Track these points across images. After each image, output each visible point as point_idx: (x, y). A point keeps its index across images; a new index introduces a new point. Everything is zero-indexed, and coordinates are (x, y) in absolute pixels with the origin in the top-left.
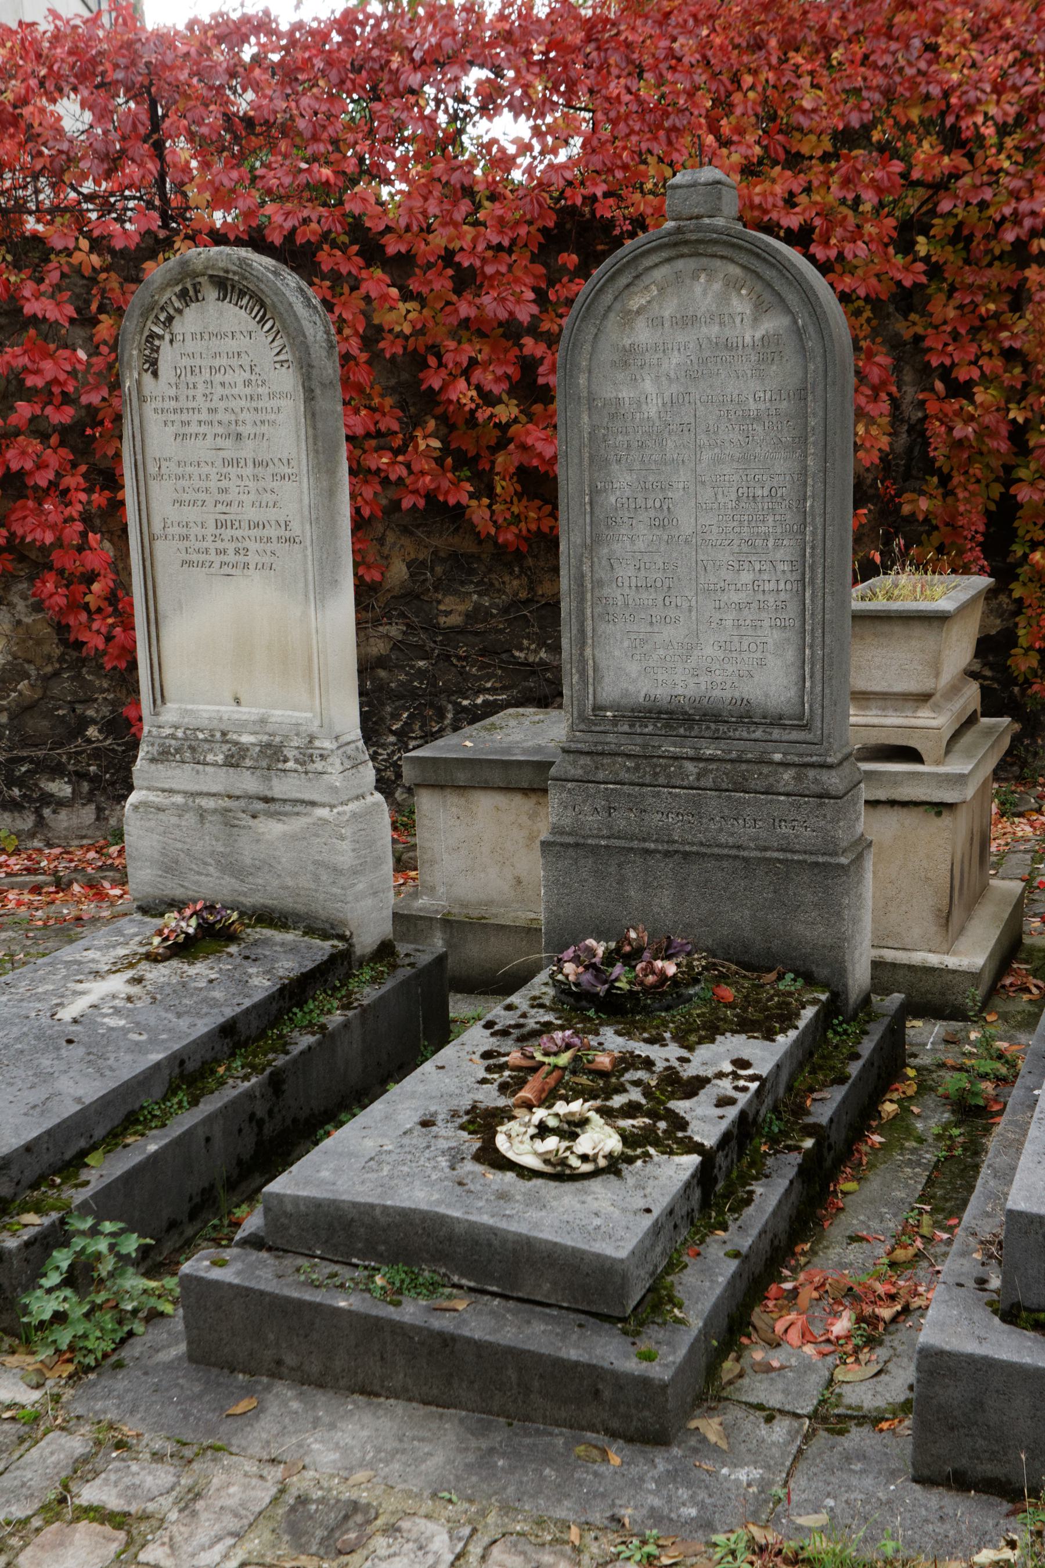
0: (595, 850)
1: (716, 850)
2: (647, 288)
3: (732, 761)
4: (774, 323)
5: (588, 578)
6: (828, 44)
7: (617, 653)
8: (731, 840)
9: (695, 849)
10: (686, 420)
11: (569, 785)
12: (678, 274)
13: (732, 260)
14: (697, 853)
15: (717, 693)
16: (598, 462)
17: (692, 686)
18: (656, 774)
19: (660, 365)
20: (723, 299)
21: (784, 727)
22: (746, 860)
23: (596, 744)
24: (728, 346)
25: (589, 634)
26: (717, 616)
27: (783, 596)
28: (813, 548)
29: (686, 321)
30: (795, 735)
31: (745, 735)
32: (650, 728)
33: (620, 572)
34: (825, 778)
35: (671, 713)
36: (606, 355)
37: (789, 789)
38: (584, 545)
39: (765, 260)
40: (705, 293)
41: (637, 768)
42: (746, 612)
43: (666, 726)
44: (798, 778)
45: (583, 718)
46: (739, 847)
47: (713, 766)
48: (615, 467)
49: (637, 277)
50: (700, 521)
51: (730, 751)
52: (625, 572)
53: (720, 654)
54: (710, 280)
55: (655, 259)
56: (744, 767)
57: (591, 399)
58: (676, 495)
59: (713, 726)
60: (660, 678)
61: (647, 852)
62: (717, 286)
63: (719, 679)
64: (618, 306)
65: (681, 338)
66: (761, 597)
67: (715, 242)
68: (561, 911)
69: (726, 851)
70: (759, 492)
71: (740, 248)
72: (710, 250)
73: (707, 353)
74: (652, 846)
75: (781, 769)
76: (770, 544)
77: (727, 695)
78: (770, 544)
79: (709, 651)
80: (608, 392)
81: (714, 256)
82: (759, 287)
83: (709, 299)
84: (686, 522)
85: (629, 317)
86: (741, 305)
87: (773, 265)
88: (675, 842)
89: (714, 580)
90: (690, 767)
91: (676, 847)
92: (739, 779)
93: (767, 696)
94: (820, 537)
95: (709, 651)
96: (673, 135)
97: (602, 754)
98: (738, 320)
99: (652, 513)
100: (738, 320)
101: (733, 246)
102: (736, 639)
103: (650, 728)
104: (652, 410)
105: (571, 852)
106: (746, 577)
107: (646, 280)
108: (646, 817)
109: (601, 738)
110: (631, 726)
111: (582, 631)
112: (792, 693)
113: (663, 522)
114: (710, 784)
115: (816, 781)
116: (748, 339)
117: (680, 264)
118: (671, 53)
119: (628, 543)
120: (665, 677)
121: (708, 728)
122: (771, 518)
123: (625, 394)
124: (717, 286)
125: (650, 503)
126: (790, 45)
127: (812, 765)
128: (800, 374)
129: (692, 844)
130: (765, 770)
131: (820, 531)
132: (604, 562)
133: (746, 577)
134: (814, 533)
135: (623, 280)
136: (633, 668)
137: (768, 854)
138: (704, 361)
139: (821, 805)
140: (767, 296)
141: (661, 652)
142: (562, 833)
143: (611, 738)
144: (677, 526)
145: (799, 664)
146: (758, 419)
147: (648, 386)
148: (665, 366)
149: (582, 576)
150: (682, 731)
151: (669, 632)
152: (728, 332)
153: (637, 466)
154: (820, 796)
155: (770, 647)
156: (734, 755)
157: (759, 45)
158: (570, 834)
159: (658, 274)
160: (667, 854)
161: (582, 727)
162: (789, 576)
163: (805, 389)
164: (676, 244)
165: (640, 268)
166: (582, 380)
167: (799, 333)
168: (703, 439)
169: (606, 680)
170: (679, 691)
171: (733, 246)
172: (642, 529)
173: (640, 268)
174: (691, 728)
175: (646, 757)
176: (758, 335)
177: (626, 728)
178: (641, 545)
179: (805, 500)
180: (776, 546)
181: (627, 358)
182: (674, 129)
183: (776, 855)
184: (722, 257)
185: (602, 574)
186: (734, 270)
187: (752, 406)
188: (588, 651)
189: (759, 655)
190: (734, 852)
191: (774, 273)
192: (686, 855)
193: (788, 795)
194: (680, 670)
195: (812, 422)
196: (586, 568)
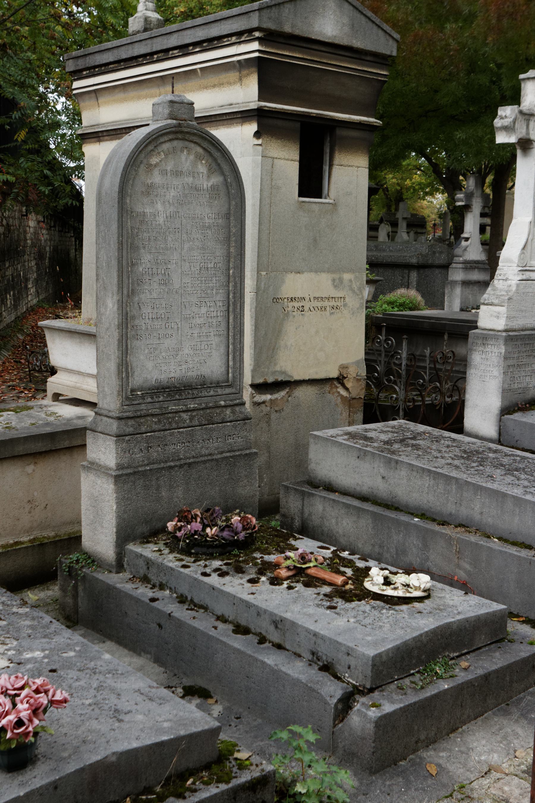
0: (144, 474)
1: (203, 459)
2: (159, 153)
3: (203, 409)
4: (216, 180)
7: (142, 357)
8: (207, 452)
9: (192, 460)
10: (177, 226)
11: (127, 438)
14: (194, 462)
15: (190, 374)
18: (170, 423)
19: (165, 196)
20: (194, 164)
21: (221, 387)
22: (217, 460)
23: (136, 411)
24: (197, 189)
27: (220, 319)
28: (234, 293)
29: (177, 173)
30: (228, 391)
34: (243, 410)
35: (168, 388)
36: (139, 188)
37: (231, 418)
39: (216, 147)
41: (159, 421)
43: (169, 395)
44: (233, 412)
46: (210, 455)
48: (142, 251)
50: (184, 281)
51: (201, 404)
52: (146, 310)
53: (192, 352)
56: (208, 411)
58: (172, 267)
60: (163, 369)
61: (171, 467)
63: (191, 366)
65: (176, 182)
66: (210, 320)
67: (194, 134)
68: (126, 516)
69: (206, 458)
71: (206, 139)
72: (192, 138)
73: (187, 192)
74: (172, 464)
75: (224, 410)
77: (194, 374)
78: (214, 292)
79: (186, 351)
80: (139, 209)
81: (191, 141)
82: (210, 160)
83: (188, 164)
85: (150, 168)
86: (202, 168)
88: (181, 459)
89: (189, 312)
90: (185, 416)
91: (182, 462)
92: (209, 417)
93: (212, 372)
94: (239, 288)
95: (186, 351)
97: (140, 417)
99: (160, 277)
101: (203, 138)
102: (199, 343)
103: (161, 398)
104: (161, 220)
105: (132, 478)
106: (204, 310)
108: (167, 448)
110: (152, 398)
112: (223, 369)
113: (166, 282)
114: (197, 423)
115: (241, 412)
116: (205, 186)
117: (175, 143)
119: (148, 293)
120: (166, 368)
121: (189, 393)
123: (148, 210)
124: (192, 157)
128: (227, 206)
129: (189, 458)
131: (238, 285)
133: (204, 310)
134: (235, 286)
135: (150, 148)
136: (150, 365)
137: (225, 455)
138: (186, 196)
139: (245, 423)
140: (214, 165)
142: (122, 468)
143: (143, 407)
144: (172, 284)
145: (226, 353)
146: (209, 227)
147: (159, 206)
148: (168, 197)
150: (177, 397)
151: (168, 343)
154: (244, 420)
155: (214, 346)
156: (204, 406)
158: (127, 468)
159: (166, 146)
160: (181, 466)
161: (127, 403)
162: (222, 309)
163: (229, 214)
169: (136, 373)
170: (172, 375)
172: (155, 286)
174: (180, 395)
175: (162, 414)
176: (210, 185)
177: (149, 400)
178: (155, 295)
183: (228, 454)
184: (195, 143)
185: (135, 312)
186: (200, 150)
187: (207, 221)
189: (209, 351)
190: (209, 458)
192: (190, 464)
193: (231, 422)
194: (172, 364)
195: (233, 230)
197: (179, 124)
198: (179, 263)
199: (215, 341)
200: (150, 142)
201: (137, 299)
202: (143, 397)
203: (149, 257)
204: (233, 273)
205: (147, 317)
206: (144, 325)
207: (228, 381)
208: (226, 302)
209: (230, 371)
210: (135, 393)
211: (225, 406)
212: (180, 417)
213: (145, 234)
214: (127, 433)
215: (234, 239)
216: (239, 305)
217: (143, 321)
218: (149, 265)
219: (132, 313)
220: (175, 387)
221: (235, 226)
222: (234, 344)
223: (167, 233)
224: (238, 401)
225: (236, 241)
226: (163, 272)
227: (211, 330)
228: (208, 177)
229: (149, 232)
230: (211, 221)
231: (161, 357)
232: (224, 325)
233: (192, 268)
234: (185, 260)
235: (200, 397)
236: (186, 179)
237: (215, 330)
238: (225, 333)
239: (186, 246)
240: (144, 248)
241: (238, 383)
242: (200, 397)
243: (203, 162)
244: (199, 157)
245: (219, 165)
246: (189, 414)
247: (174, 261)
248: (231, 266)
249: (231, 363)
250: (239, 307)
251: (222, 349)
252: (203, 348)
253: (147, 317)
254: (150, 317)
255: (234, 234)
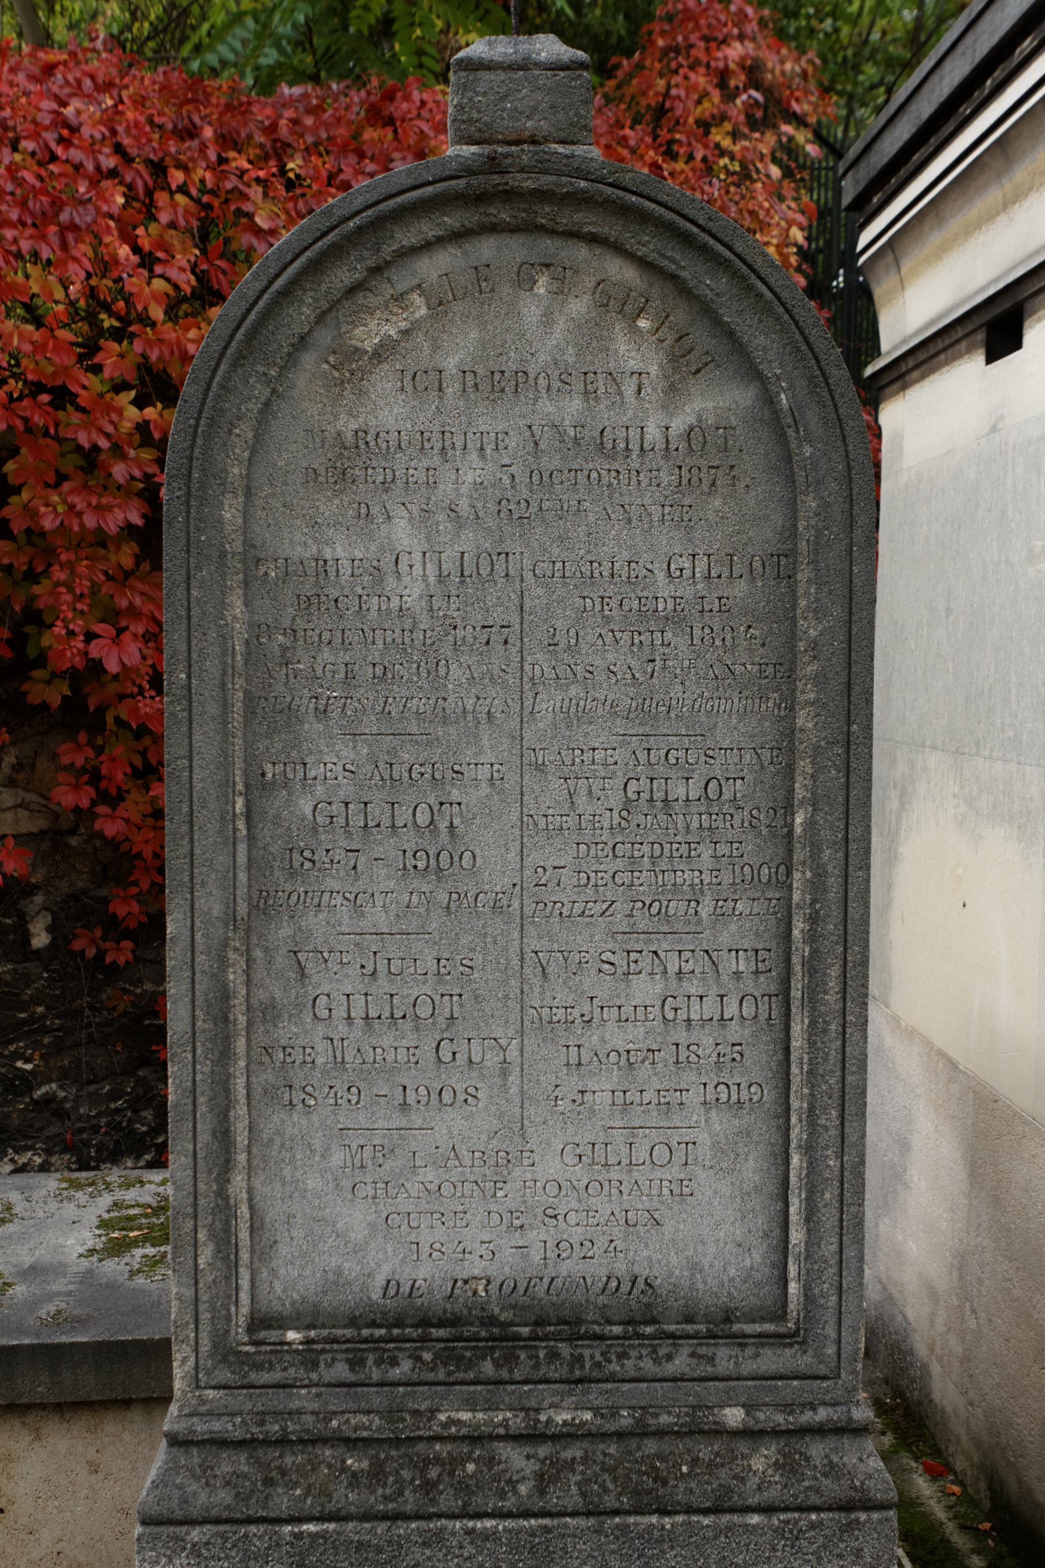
2: (399, 298)
3: (620, 1435)
4: (716, 401)
5: (239, 1002)
6: (280, 150)
7: (312, 1183)
10: (497, 616)
11: (195, 1534)
12: (480, 272)
13: (618, 249)
15: (570, 1267)
16: (268, 714)
17: (507, 1254)
18: (429, 1487)
19: (432, 485)
20: (591, 335)
21: (740, 1340)
24: (602, 446)
25: (241, 1139)
26: (572, 1083)
27: (735, 1032)
28: (813, 919)
29: (499, 383)
30: (770, 1360)
31: (648, 1366)
32: (404, 1368)
33: (321, 982)
34: (851, 1460)
35: (454, 1321)
37: (772, 1494)
38: (231, 919)
40: (548, 319)
41: (377, 1473)
42: (644, 1072)
43: (445, 1357)
44: (789, 1467)
45: (224, 1352)
47: (573, 1452)
48: (312, 727)
49: (377, 270)
50: (534, 858)
51: (614, 1413)
52: (337, 984)
53: (580, 1175)
54: (559, 292)
55: (426, 228)
56: (651, 1446)
57: (253, 557)
58: (472, 796)
59: (564, 1349)
60: (426, 1238)
62: (578, 306)
63: (576, 1234)
64: (324, 337)
66: (681, 1036)
67: (581, 200)
70: (679, 791)
71: (644, 218)
72: (569, 218)
73: (550, 462)
76: (705, 912)
77: (597, 1270)
78: (705, 912)
79: (551, 1167)
80: (296, 544)
81: (573, 235)
82: (681, 315)
83: (558, 334)
84: (495, 859)
85: (352, 368)
86: (636, 353)
87: (724, 265)
89: (563, 997)
90: (516, 1459)
93: (694, 1267)
94: (833, 894)
95: (551, 1167)
96: (70, 237)
97: (282, 1442)
98: (629, 389)
99: (409, 840)
100: (629, 389)
101: (625, 211)
102: (619, 1137)
103: (404, 1368)
104: (411, 590)
106: (646, 989)
107: (401, 279)
109: (277, 1400)
110: (355, 1364)
111: (224, 1135)
112: (757, 1257)
113: (438, 859)
114: (573, 1499)
115: (832, 1470)
116: (653, 433)
117: (486, 248)
118: (60, 121)
119: (344, 912)
120: (440, 1234)
121: (554, 1355)
122: (706, 852)
123: (340, 549)
124: (578, 306)
125: (403, 815)
126: (228, 141)
127: (819, 1431)
128: (778, 519)
130: (705, 1452)
131: (833, 882)
132: (281, 960)
133: (646, 989)
134: (817, 887)
135: (342, 276)
136: (356, 1219)
138: (544, 480)
139: (850, 1527)
140: (702, 338)
141: (429, 1175)
143: (302, 1399)
144: (473, 871)
145: (772, 1187)
146: (677, 618)
147: (402, 532)
148: (446, 488)
149: (226, 996)
150: (488, 1368)
151: (448, 1126)
152: (605, 415)
153: (370, 724)
154: (847, 1507)
155: (705, 1152)
156: (625, 1419)
157: (191, 132)
159: (431, 267)
161: (224, 1375)
162: (749, 985)
163: (792, 553)
164: (481, 198)
165: (387, 250)
166: (230, 512)
167: (776, 423)
168: (540, 661)
169: (283, 1249)
170: (476, 1267)
171: (625, 211)
172: (383, 878)
173: (387, 250)
174: (510, 1360)
175: (397, 1442)
176: (678, 425)
177: (341, 1371)
178: (378, 917)
179: (789, 809)
180: (719, 916)
181: (347, 463)
182: (73, 227)
184: (593, 239)
186: (620, 271)
187: (663, 587)
188: (238, 1182)
189: (675, 1172)
191: (723, 283)
193: (767, 1510)
195: (811, 629)
196: (234, 977)
197: (492, 158)
198: (512, 780)
199: (707, 1130)
200: (335, 253)
201: (285, 932)
202: (309, 1356)
203: (348, 754)
204: (810, 824)
205: (340, 1012)
206: (321, 1046)
207: (780, 1313)
208: (772, 959)
209: (792, 1270)
210: (273, 1335)
211: (751, 1434)
212: (491, 1461)
213: (326, 655)
214: (195, 1513)
215: (812, 669)
216: (834, 972)
217: (320, 1030)
218: (346, 789)
219: (261, 995)
220: (492, 1321)
221: (818, 613)
222: (809, 1149)
223: (446, 650)
224: (822, 1414)
225: (820, 680)
226: (423, 818)
227: (689, 1078)
228: (672, 389)
229: (346, 645)
230: (687, 591)
231: (414, 1188)
232: (759, 1059)
233: (582, 800)
234: (540, 768)
235: (612, 1378)
236: (546, 406)
237: (712, 1079)
238: (769, 1096)
239: (548, 703)
240: (322, 713)
241: (831, 1331)
242: (612, 1378)
243: (643, 324)
244: (615, 304)
245: (730, 334)
246: (543, 1451)
247: (484, 772)
248: (800, 793)
249: (797, 1236)
250: (833, 985)
251: (752, 1168)
252: (641, 1154)
253: (340, 1012)
254: (358, 1013)
255: (814, 645)
